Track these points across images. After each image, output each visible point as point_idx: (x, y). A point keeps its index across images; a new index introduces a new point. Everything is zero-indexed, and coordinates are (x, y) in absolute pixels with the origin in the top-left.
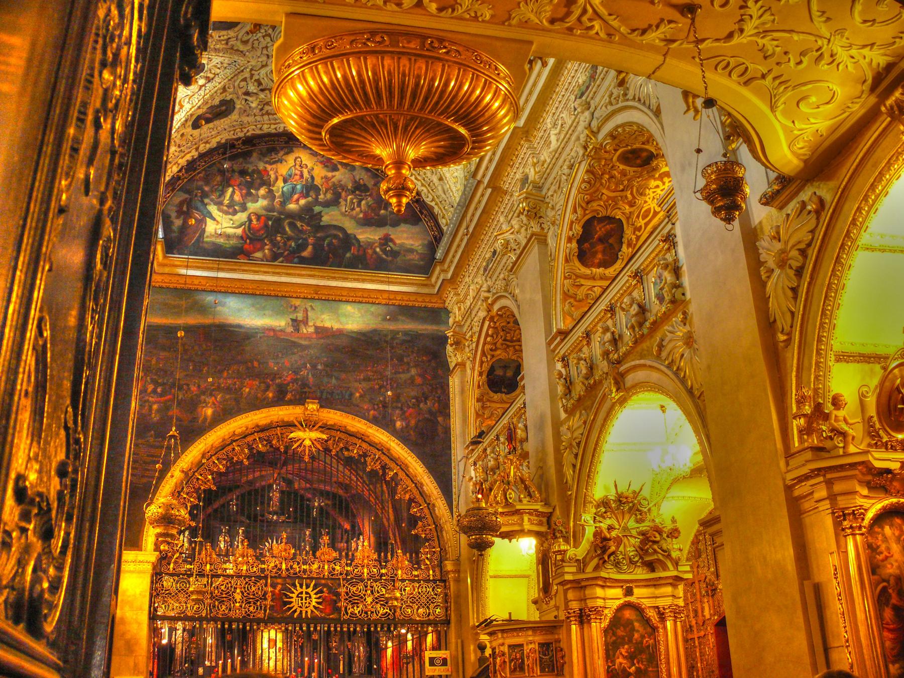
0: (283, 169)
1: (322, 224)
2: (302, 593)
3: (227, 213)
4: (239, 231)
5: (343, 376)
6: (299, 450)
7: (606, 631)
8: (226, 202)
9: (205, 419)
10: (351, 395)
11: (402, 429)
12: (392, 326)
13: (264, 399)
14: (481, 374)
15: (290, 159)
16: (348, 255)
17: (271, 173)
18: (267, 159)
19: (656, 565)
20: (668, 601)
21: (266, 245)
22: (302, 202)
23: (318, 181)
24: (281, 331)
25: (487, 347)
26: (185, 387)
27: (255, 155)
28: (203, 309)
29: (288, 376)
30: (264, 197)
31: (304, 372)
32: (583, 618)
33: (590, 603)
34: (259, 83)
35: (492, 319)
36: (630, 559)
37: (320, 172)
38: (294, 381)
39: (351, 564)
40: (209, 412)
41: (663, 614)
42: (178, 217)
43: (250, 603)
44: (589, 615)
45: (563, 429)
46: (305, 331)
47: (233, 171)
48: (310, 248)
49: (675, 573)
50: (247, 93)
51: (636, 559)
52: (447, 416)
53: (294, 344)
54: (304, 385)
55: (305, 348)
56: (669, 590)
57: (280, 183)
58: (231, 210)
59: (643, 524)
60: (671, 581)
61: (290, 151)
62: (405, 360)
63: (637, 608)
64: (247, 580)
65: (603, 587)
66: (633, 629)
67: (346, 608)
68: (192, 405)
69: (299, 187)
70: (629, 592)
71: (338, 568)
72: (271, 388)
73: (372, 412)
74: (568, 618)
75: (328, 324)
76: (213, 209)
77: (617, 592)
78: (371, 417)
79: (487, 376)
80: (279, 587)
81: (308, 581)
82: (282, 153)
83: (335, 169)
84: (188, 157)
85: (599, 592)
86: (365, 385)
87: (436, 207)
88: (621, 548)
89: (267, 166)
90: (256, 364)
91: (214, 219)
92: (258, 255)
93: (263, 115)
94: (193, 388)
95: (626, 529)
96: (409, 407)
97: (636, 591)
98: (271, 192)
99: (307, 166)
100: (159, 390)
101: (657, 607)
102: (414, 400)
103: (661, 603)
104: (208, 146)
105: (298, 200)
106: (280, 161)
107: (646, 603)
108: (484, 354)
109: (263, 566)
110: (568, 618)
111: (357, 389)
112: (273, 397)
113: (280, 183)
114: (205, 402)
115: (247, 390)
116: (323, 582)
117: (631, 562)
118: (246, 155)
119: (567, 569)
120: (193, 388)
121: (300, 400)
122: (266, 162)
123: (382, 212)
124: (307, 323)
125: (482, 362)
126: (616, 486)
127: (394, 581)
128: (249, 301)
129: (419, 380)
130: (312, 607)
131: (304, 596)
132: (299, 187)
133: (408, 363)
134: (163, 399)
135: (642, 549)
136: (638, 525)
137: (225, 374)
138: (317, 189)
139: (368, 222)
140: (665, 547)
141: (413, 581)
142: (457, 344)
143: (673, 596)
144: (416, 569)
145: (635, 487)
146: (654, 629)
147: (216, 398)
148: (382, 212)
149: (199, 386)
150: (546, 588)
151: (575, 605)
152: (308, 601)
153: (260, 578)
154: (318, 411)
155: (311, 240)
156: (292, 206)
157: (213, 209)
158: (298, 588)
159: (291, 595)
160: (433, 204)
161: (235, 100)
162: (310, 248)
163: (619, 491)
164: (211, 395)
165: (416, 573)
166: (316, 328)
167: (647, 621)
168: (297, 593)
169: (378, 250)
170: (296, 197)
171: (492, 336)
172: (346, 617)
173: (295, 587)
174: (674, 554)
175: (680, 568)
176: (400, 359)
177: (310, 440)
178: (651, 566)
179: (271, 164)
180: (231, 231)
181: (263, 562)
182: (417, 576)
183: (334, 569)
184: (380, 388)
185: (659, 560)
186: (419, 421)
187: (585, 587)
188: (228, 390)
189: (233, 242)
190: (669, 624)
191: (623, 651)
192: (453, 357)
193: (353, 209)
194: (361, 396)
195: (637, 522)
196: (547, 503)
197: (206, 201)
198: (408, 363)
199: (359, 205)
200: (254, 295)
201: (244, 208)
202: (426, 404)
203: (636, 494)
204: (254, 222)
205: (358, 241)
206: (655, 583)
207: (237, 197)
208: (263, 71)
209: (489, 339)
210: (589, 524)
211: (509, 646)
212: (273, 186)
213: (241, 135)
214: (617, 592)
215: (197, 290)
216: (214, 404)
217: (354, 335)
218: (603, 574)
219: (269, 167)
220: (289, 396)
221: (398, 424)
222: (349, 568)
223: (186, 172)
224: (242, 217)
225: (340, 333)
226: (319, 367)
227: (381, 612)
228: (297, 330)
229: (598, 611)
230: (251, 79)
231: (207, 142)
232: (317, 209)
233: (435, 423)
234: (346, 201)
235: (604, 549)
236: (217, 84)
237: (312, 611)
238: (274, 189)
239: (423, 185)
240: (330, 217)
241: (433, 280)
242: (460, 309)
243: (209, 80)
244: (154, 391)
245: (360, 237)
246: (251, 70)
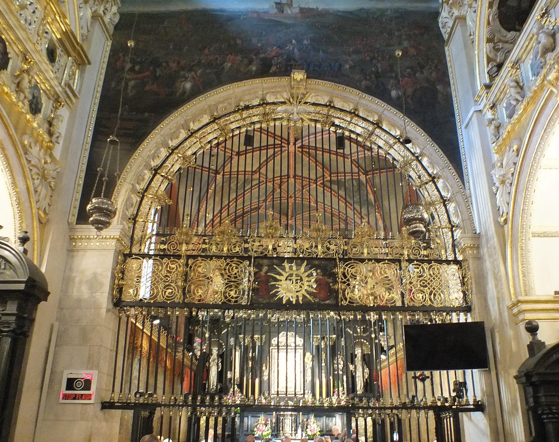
2: (291, 275)
5: (331, 50)
9: (184, 92)
10: (340, 65)
11: (399, 98)
13: (248, 72)
24: (265, 12)
26: (164, 64)
29: (272, 51)
31: (289, 47)
39: (346, 244)
40: (188, 85)
43: (231, 286)
46: (289, 12)
52: (447, 84)
53: (278, 23)
55: (287, 26)
64: (228, 260)
67: (344, 291)
68: (172, 79)
71: (332, 247)
72: (255, 62)
73: (364, 83)
75: (313, 6)
78: (363, 87)
80: (265, 269)
81: (299, 261)
86: (354, 56)
90: (239, 42)
94: (173, 65)
96: (403, 76)
100: (137, 68)
102: (408, 70)
109: (247, 246)
111: (346, 62)
112: (257, 70)
114: (184, 76)
115: (229, 64)
116: (316, 262)
120: (173, 65)
121: (285, 72)
124: (292, 5)
127: (399, 261)
129: (412, 51)
130: (303, 292)
131: (294, 278)
133: (400, 36)
134: (139, 76)
137: (206, 51)
141: (423, 261)
144: (425, 248)
147: (196, 73)
149: (179, 63)
152: (299, 284)
153: (243, 258)
158: (287, 269)
159: (277, 277)
164: (191, 70)
165: (425, 253)
168: (285, 275)
172: (344, 303)
173: (284, 269)
176: (390, 34)
181: (246, 242)
182: (427, 256)
183: (328, 249)
184: (371, 60)
186: (416, 90)
188: (209, 65)
194: (350, 68)
198: (400, 36)
216: (193, 78)
217: (340, 14)
220: (273, 69)
221: (394, 93)
222: (346, 248)
225: (324, 14)
226: (305, 42)
227: (386, 297)
233: (435, 92)
237: (304, 296)
244: (132, 70)
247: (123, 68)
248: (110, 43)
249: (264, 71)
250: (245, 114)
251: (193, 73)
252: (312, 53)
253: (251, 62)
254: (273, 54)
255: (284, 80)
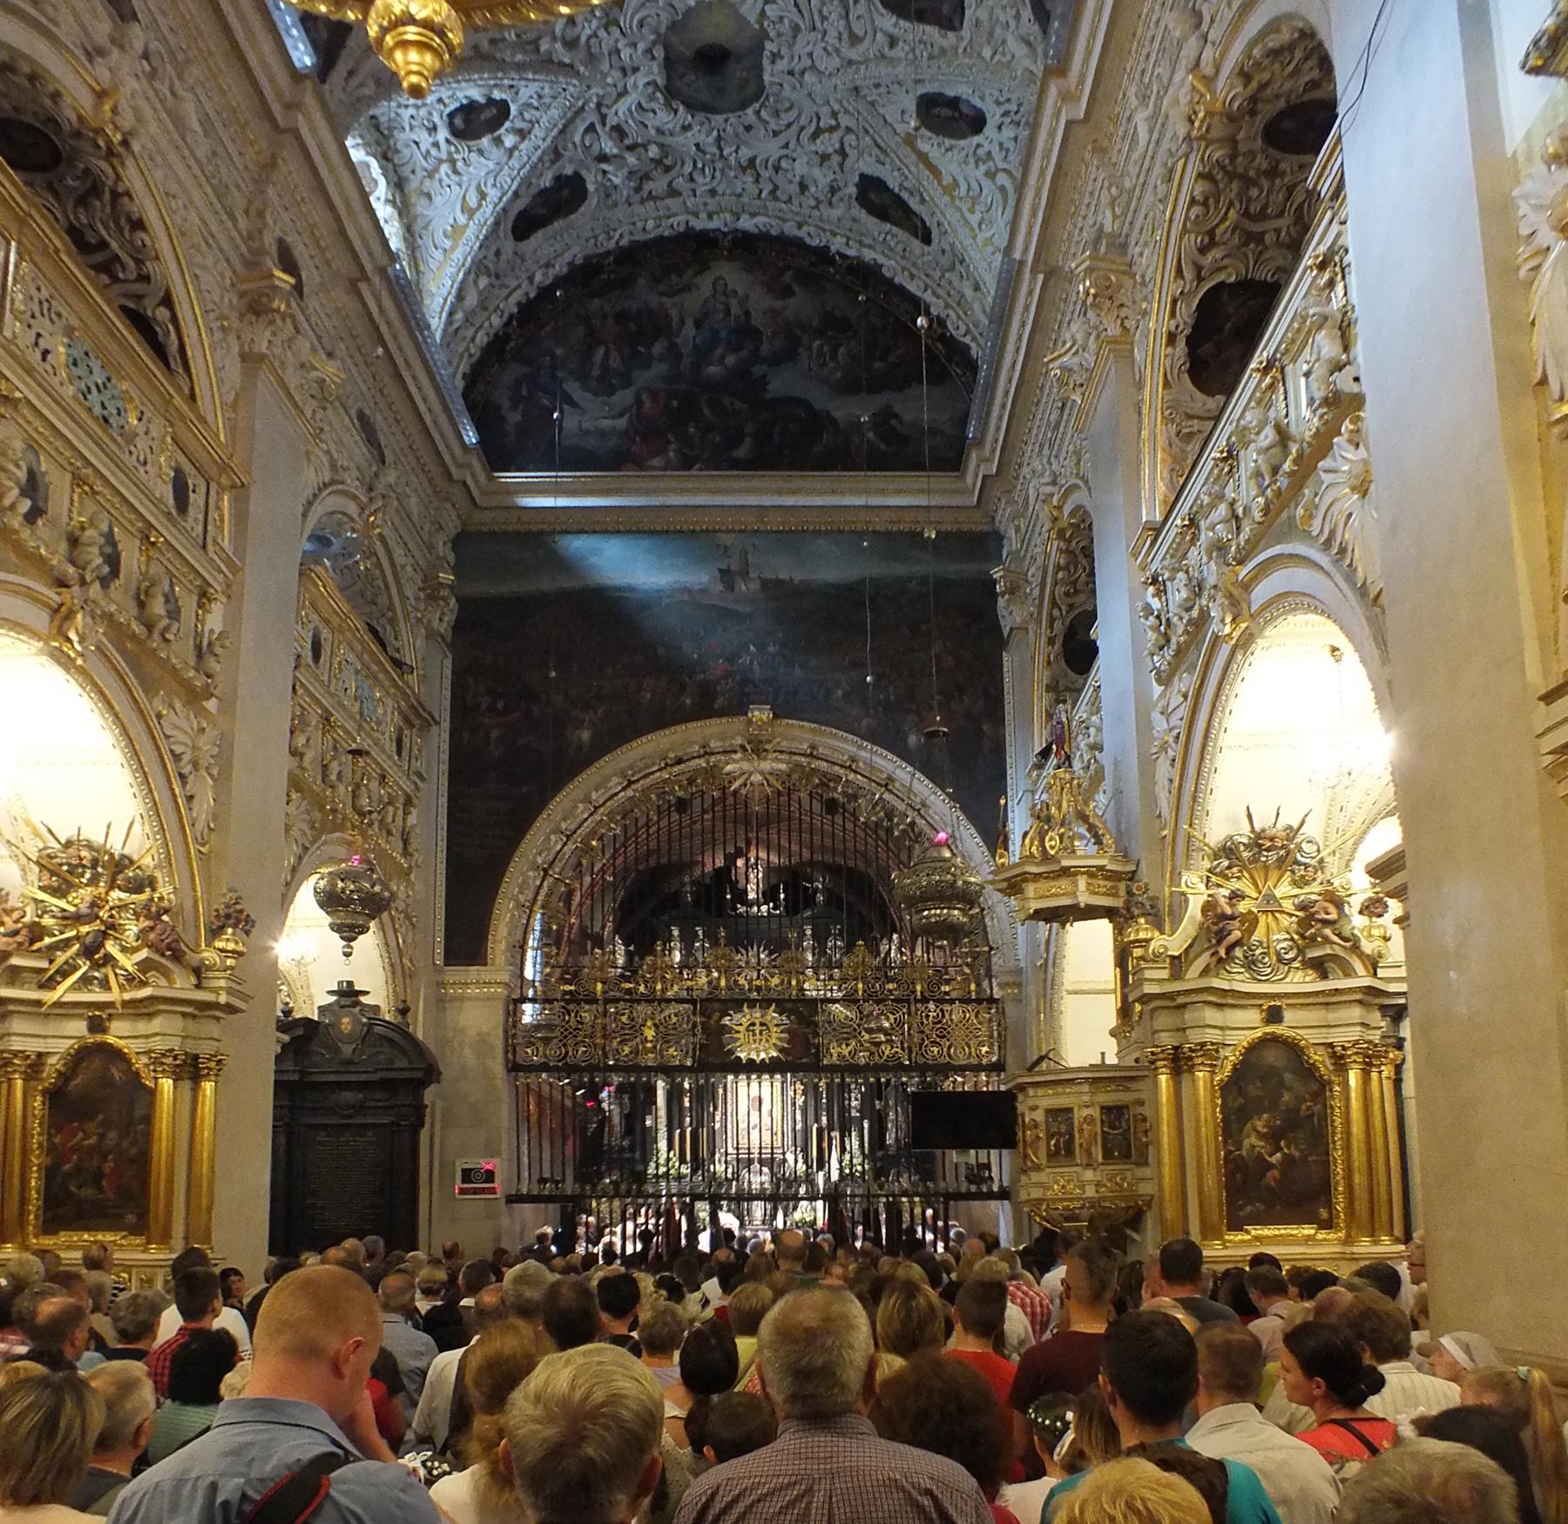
0: (692, 303)
1: (769, 396)
3: (596, 393)
4: (622, 423)
6: (743, 792)
7: (1225, 1088)
8: (596, 372)
12: (900, 570)
14: (1051, 641)
15: (705, 284)
16: (817, 449)
17: (674, 313)
18: (663, 288)
19: (1330, 965)
20: (1355, 1033)
21: (669, 442)
22: (731, 360)
23: (757, 320)
24: (703, 591)
25: (1060, 590)
27: (642, 281)
28: (564, 564)
29: (717, 667)
30: (661, 358)
31: (745, 660)
32: (1180, 1063)
33: (1195, 1037)
34: (619, 131)
35: (1061, 534)
36: (1278, 954)
37: (760, 302)
38: (728, 675)
40: (586, 736)
41: (1342, 1057)
42: (514, 408)
44: (1191, 1059)
45: (1156, 716)
47: (605, 316)
48: (748, 442)
49: (1368, 982)
50: (603, 158)
51: (1291, 955)
54: (746, 681)
56: (1356, 1013)
57: (689, 330)
58: (605, 385)
59: (1307, 889)
60: (1359, 997)
61: (706, 268)
62: (923, 628)
63: (1293, 1049)
65: (1220, 1006)
66: (1281, 1085)
69: (723, 334)
70: (1274, 1016)
74: (1153, 1063)
76: (573, 388)
77: (1252, 1017)
79: (1064, 645)
82: (689, 272)
83: (787, 292)
84: (517, 296)
85: (1211, 1016)
87: (973, 345)
88: (1258, 935)
89: (665, 299)
90: (661, 651)
91: (574, 404)
92: (656, 462)
93: (642, 201)
95: (1270, 898)
97: (1288, 1016)
98: (673, 347)
99: (735, 292)
101: (1331, 1045)
103: (1340, 1037)
104: (552, 273)
105: (723, 357)
106: (688, 288)
107: (1309, 1037)
108: (1054, 603)
110: (1153, 1063)
111: (837, 684)
113: (689, 330)
117: (1280, 960)
118: (625, 283)
119: (1148, 974)
121: (738, 708)
122: (662, 294)
123: (877, 365)
125: (1052, 620)
126: (1250, 817)
128: (645, 543)
132: (723, 334)
135: (1303, 937)
136: (1296, 891)
138: (756, 334)
139: (850, 386)
140: (1347, 934)
142: (1012, 590)
143: (1363, 1024)
145: (1290, 818)
146: (1321, 1088)
148: (877, 365)
150: (1125, 1012)
151: (1167, 1040)
154: (771, 723)
155: (749, 428)
156: (713, 370)
157: (573, 388)
160: (967, 340)
161: (584, 173)
162: (748, 442)
163: (1258, 828)
166: (765, 584)
167: (1308, 1072)
169: (871, 435)
170: (719, 351)
171: (1066, 568)
174: (1367, 947)
175: (1380, 973)
177: (762, 773)
178: (1320, 967)
179: (670, 295)
180: (606, 423)
185: (1334, 958)
187: (1184, 1006)
189: (612, 443)
190: (1354, 1077)
191: (1260, 1125)
192: (1010, 614)
193: (824, 365)
195: (1295, 883)
196: (1126, 856)
197: (560, 374)
199: (834, 357)
200: (652, 533)
201: (628, 383)
202: (961, 702)
203: (1292, 833)
204: (647, 405)
205: (834, 421)
206: (1328, 1000)
207: (615, 362)
208: (622, 107)
209: (1060, 575)
210: (1195, 889)
211: (1052, 1113)
212: (678, 335)
213: (612, 245)
214: (1252, 1017)
215: (553, 532)
218: (1217, 983)
219: (668, 302)
220: (720, 702)
221: (912, 740)
223: (521, 325)
224: (624, 397)
226: (771, 649)
228: (730, 587)
229: (1210, 1052)
230: (604, 124)
231: (548, 265)
232: (758, 370)
234: (810, 349)
235: (1221, 936)
236: (540, 139)
238: (678, 341)
239: (947, 306)
240: (781, 383)
241: (969, 480)
242: (1018, 529)
243: (523, 134)
244: (492, 709)
245: (835, 414)
246: (599, 105)
247: (478, 706)
248: (448, 662)
249: (705, 708)
250: (676, 769)
251: (591, 712)
252: (782, 670)
253: (682, 690)
254: (719, 673)
255: (737, 723)
